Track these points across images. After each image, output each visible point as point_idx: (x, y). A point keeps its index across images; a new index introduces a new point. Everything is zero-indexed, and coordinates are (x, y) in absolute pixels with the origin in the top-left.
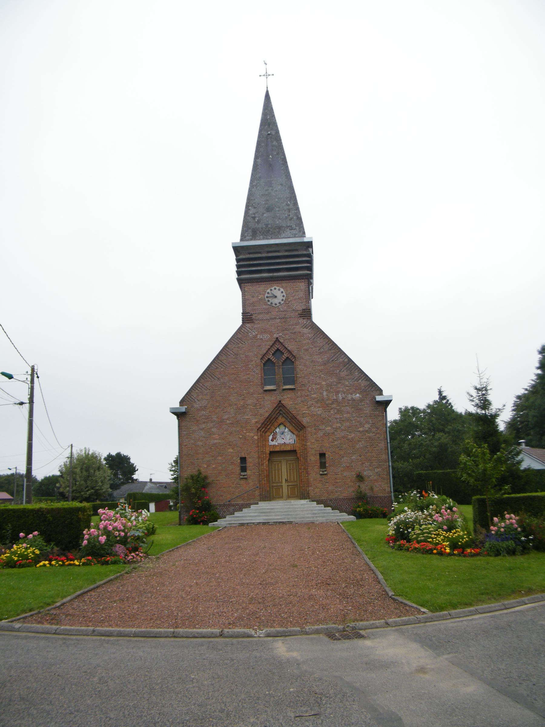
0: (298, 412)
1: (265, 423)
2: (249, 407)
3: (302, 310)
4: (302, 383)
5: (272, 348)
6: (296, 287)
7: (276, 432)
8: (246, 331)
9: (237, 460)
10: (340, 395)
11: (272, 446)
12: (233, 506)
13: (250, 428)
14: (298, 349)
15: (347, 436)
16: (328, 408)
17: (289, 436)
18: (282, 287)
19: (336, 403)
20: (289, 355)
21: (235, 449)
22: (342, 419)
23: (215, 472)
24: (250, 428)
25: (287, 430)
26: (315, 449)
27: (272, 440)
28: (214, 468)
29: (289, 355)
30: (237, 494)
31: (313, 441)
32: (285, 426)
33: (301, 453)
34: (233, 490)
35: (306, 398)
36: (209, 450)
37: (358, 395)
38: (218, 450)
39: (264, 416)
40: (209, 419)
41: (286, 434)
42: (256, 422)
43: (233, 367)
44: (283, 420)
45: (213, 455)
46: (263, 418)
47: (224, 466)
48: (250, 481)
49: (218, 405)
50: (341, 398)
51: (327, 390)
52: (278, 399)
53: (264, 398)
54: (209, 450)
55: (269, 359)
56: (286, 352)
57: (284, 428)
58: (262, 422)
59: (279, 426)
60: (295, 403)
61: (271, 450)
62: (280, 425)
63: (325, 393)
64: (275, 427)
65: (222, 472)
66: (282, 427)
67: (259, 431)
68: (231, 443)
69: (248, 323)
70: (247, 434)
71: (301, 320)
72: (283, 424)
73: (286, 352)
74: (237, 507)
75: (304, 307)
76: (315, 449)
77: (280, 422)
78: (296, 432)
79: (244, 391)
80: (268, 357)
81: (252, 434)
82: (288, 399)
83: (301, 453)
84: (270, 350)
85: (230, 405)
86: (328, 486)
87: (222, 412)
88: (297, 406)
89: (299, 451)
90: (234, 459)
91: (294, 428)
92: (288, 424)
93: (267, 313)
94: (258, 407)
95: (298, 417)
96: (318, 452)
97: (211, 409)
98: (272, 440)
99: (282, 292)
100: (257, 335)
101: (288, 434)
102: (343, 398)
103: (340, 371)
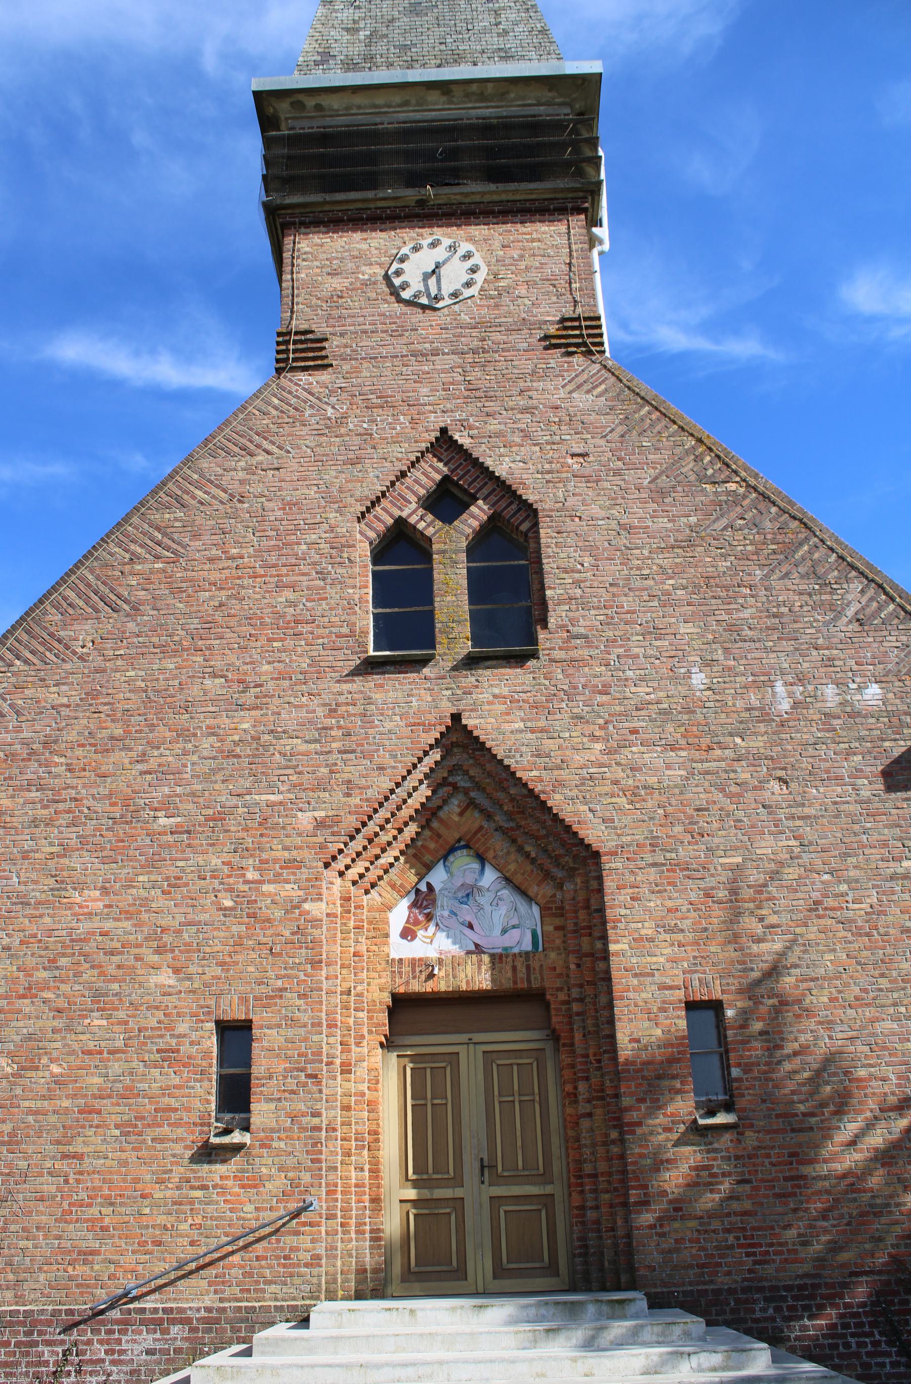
1: (372, 827)
2: (288, 744)
3: (563, 320)
4: (575, 630)
5: (416, 473)
6: (533, 241)
8: (293, 401)
9: (194, 1036)
10: (780, 688)
11: (406, 969)
12: (156, 1323)
13: (286, 854)
14: (548, 477)
15: (830, 902)
16: (718, 752)
17: (503, 909)
18: (470, 239)
19: (762, 727)
20: (503, 504)
21: (192, 969)
22: (807, 811)
23: (66, 1103)
24: (286, 854)
25: (490, 876)
26: (658, 978)
27: (407, 934)
28: (58, 1081)
29: (503, 504)
30: (182, 1250)
31: (648, 930)
32: (482, 859)
33: (576, 1007)
34: (161, 1219)
35: (600, 698)
36: (42, 974)
37: (874, 691)
38: (89, 975)
39: (370, 792)
40: (61, 806)
41: (484, 900)
42: (320, 824)
43: (214, 552)
44: (474, 820)
45: (62, 1003)
47: (116, 1067)
48: (265, 1165)
49: (119, 732)
50: (785, 705)
51: (708, 664)
52: (448, 708)
53: (369, 700)
54: (42, 974)
55: (401, 523)
56: (485, 491)
57: (476, 866)
58: (352, 821)
59: (445, 858)
60: (542, 723)
62: (452, 850)
63: (699, 679)
65: (106, 1105)
66: (463, 862)
68: (167, 939)
69: (305, 369)
70: (266, 888)
71: (555, 358)
72: (467, 847)
73: (485, 491)
74: (175, 1330)
75: (568, 312)
76: (658, 978)
77: (451, 836)
78: (547, 890)
79: (266, 668)
80: (397, 513)
81: (290, 891)
82: (501, 708)
83: (576, 1007)
84: (408, 481)
85: (183, 734)
86: (747, 1205)
87: (140, 767)
89: (562, 996)
90: (182, 1027)
91: (529, 867)
92: (498, 845)
93: (396, 334)
95: (556, 801)
96: (680, 994)
97: (79, 752)
99: (467, 256)
100: (345, 417)
101: (496, 901)
102: (796, 705)
103: (767, 577)
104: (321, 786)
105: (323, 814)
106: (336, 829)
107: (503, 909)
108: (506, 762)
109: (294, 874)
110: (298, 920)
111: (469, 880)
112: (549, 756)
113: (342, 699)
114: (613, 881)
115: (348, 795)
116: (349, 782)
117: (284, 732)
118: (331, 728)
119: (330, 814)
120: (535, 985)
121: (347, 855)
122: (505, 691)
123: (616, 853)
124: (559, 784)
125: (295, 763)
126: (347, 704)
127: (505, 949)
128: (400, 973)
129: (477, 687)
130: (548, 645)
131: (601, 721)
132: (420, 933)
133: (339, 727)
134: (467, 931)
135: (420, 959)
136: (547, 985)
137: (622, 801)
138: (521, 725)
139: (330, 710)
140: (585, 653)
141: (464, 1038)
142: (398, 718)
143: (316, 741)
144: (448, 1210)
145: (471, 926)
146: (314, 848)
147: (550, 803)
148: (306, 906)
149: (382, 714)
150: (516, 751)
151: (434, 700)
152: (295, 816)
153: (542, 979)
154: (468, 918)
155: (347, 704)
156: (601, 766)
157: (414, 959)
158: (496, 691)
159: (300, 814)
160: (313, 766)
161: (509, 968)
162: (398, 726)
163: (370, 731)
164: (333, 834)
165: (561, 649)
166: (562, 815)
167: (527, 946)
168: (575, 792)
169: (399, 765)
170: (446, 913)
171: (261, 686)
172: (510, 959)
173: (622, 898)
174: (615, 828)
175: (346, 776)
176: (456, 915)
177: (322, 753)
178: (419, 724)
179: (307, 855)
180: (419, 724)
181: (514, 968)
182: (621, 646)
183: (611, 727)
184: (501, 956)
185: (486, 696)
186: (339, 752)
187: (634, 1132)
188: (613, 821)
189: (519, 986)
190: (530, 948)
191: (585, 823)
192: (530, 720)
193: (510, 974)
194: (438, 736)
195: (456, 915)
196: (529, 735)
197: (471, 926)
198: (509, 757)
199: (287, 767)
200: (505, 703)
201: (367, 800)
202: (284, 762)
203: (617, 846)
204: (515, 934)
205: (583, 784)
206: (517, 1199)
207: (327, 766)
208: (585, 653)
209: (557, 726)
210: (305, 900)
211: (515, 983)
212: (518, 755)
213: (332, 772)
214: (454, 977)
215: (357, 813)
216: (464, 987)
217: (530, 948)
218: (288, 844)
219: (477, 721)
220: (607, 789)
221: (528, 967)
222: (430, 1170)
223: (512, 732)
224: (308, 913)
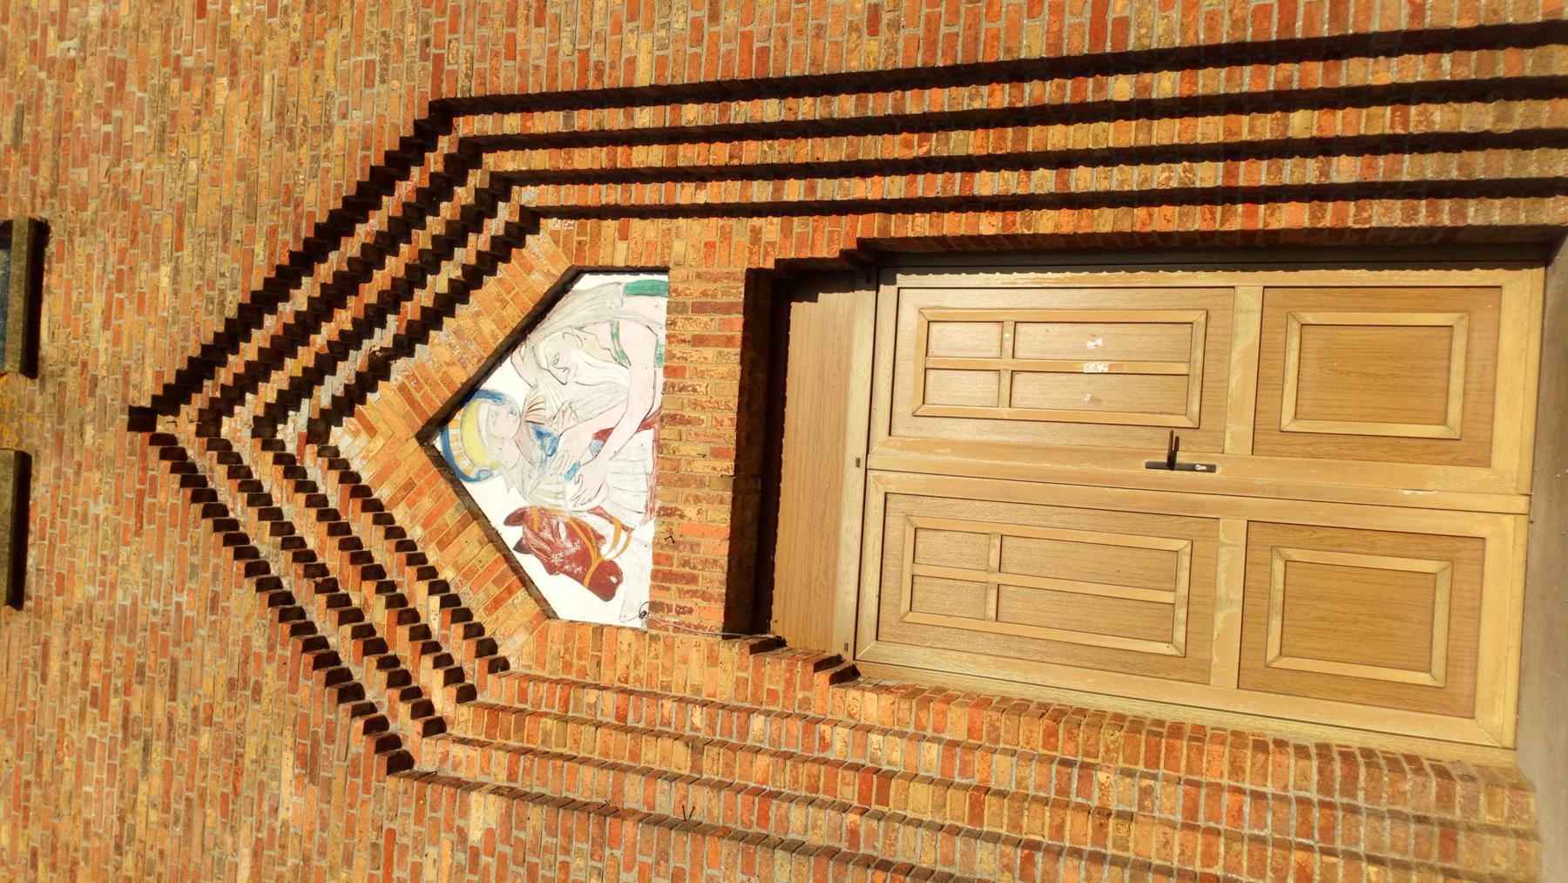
0: (265, 200)
2: (147, 818)
7: (516, 518)
11: (671, 598)
13: (362, 860)
17: (576, 357)
35: (132, 87)
39: (259, 644)
41: (553, 398)
42: (309, 763)
46: (270, 670)
58: (312, 683)
60: (169, 226)
61: (714, 615)
62: (443, 464)
64: (451, 516)
67: (426, 754)
82: (129, 318)
88: (206, 212)
94: (160, 706)
98: (604, 582)
101: (558, 370)
104: (231, 748)
105: (288, 758)
106: (322, 731)
107: (576, 357)
108: (231, 312)
109: (404, 849)
110: (503, 858)
111: (508, 426)
112: (228, 211)
113: (75, 674)
114: (495, 71)
115: (257, 690)
116: (232, 684)
117: (122, 819)
118: (127, 708)
119: (289, 742)
120: (737, 294)
121: (391, 708)
122: (98, 301)
123: (439, 60)
124: (289, 196)
125: (182, 806)
126: (86, 664)
127: (658, 358)
128: (681, 610)
129: (84, 365)
130: (26, 198)
131: (175, 84)
132: (607, 552)
133: (127, 690)
134: (613, 442)
135: (657, 559)
136: (740, 269)
137: (333, 38)
138: (166, 270)
139: (94, 705)
140: (48, 114)
141: (854, 477)
142: (124, 552)
143: (146, 750)
144: (1279, 566)
145: (604, 435)
146: (354, 794)
147: (322, 218)
148: (475, 836)
149: (113, 586)
150: (211, 284)
151: (99, 467)
152: (285, 824)
153: (729, 276)
154: (587, 437)
155: (86, 664)
156: (257, 88)
157: (655, 575)
158: (97, 323)
159: (283, 814)
160: (193, 765)
161: (695, 353)
162: (138, 553)
163: (141, 620)
164: (330, 739)
165: (35, 171)
166: (348, 190)
167: (657, 308)
168: (304, 152)
169: (213, 561)
170: (571, 488)
171: (34, 853)
172: (677, 350)
173: (535, 48)
174: (385, 59)
175: (221, 691)
176: (575, 467)
177: (170, 740)
178: (140, 506)
179: (367, 811)
180: (140, 506)
181: (698, 341)
182: (44, 34)
183: (188, 62)
184: (670, 371)
185: (102, 341)
186: (173, 698)
187: (1122, 24)
188: (370, 64)
189: (737, 332)
190: (663, 302)
191: (368, 131)
192: (156, 253)
193: (709, 352)
194: (167, 464)
195: (575, 467)
196: (186, 255)
197: (604, 435)
198: (222, 303)
199: (188, 826)
200: (121, 303)
201: (271, 648)
202: (179, 830)
203: (424, 57)
204: (629, 332)
205: (291, 133)
206: (1265, 382)
207: (195, 731)
208: (48, 114)
209: (172, 187)
210: (462, 834)
211: (729, 341)
212: (221, 282)
213: (209, 721)
214: (701, 484)
215: (294, 680)
216: (727, 465)
217: (663, 302)
218: (339, 854)
219: (149, 372)
220: (305, 73)
221: (699, 308)
222: (1167, 597)
223: (176, 293)
224: (489, 832)
